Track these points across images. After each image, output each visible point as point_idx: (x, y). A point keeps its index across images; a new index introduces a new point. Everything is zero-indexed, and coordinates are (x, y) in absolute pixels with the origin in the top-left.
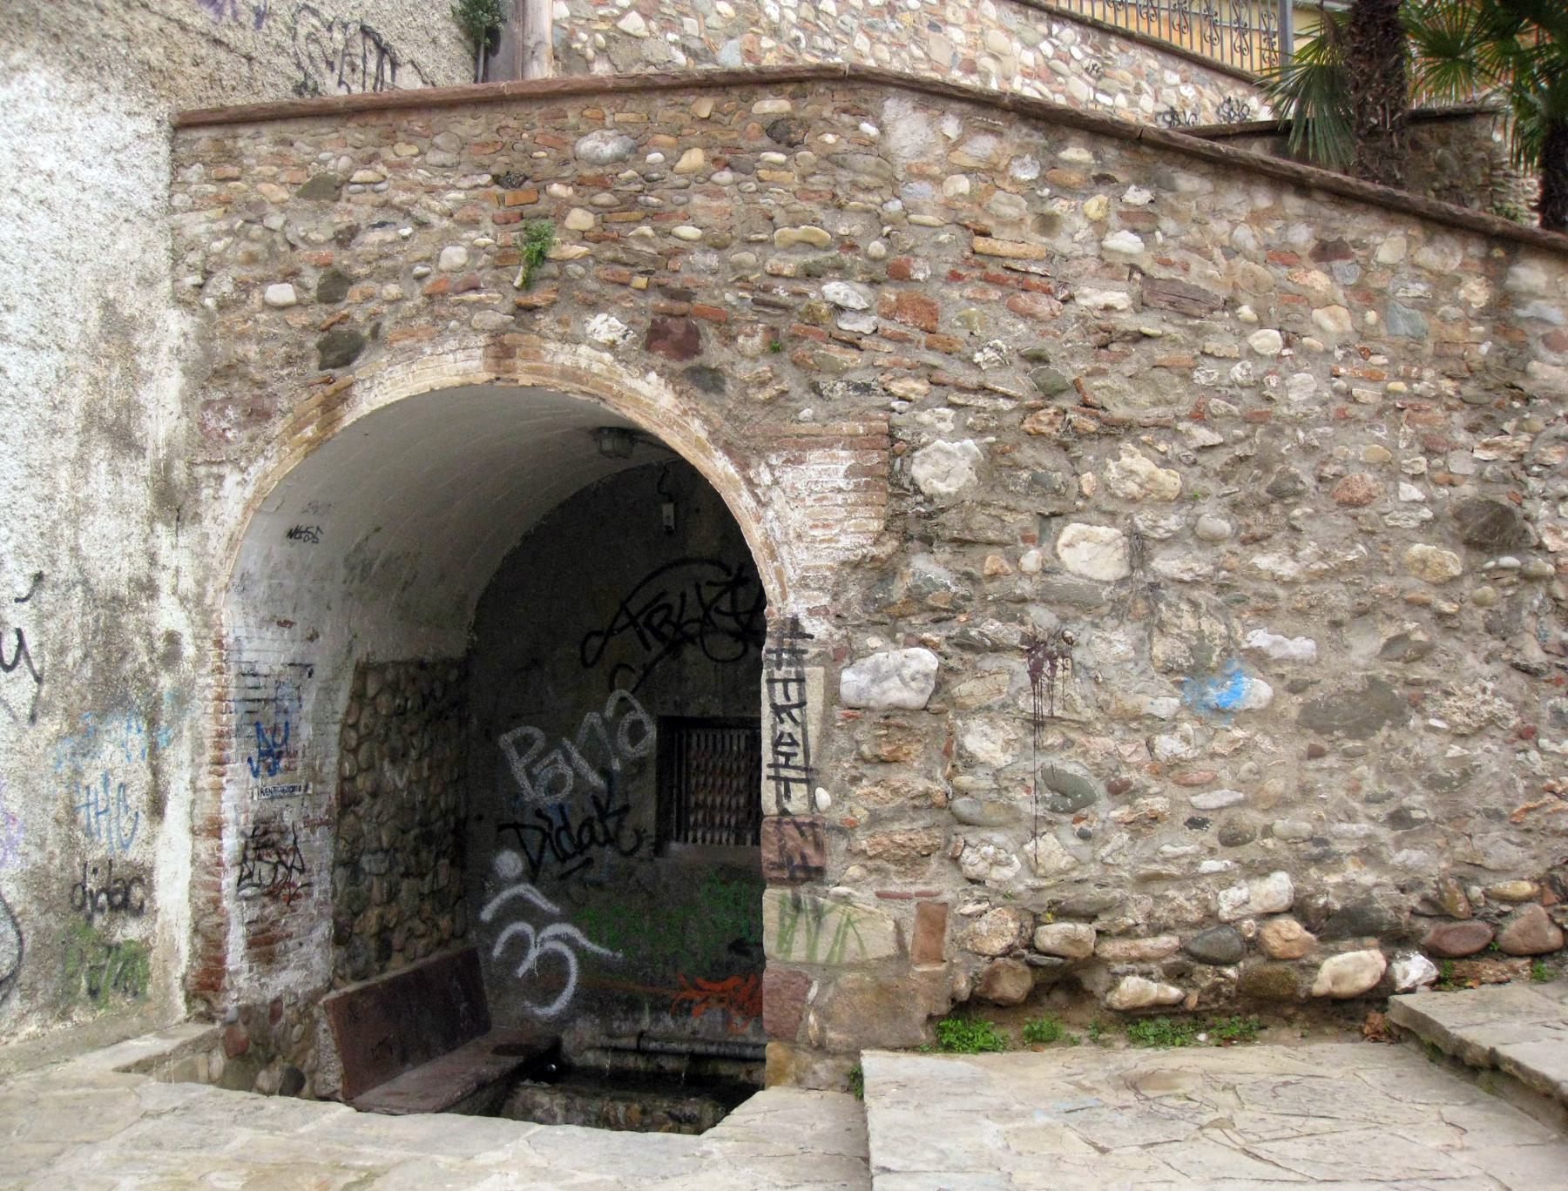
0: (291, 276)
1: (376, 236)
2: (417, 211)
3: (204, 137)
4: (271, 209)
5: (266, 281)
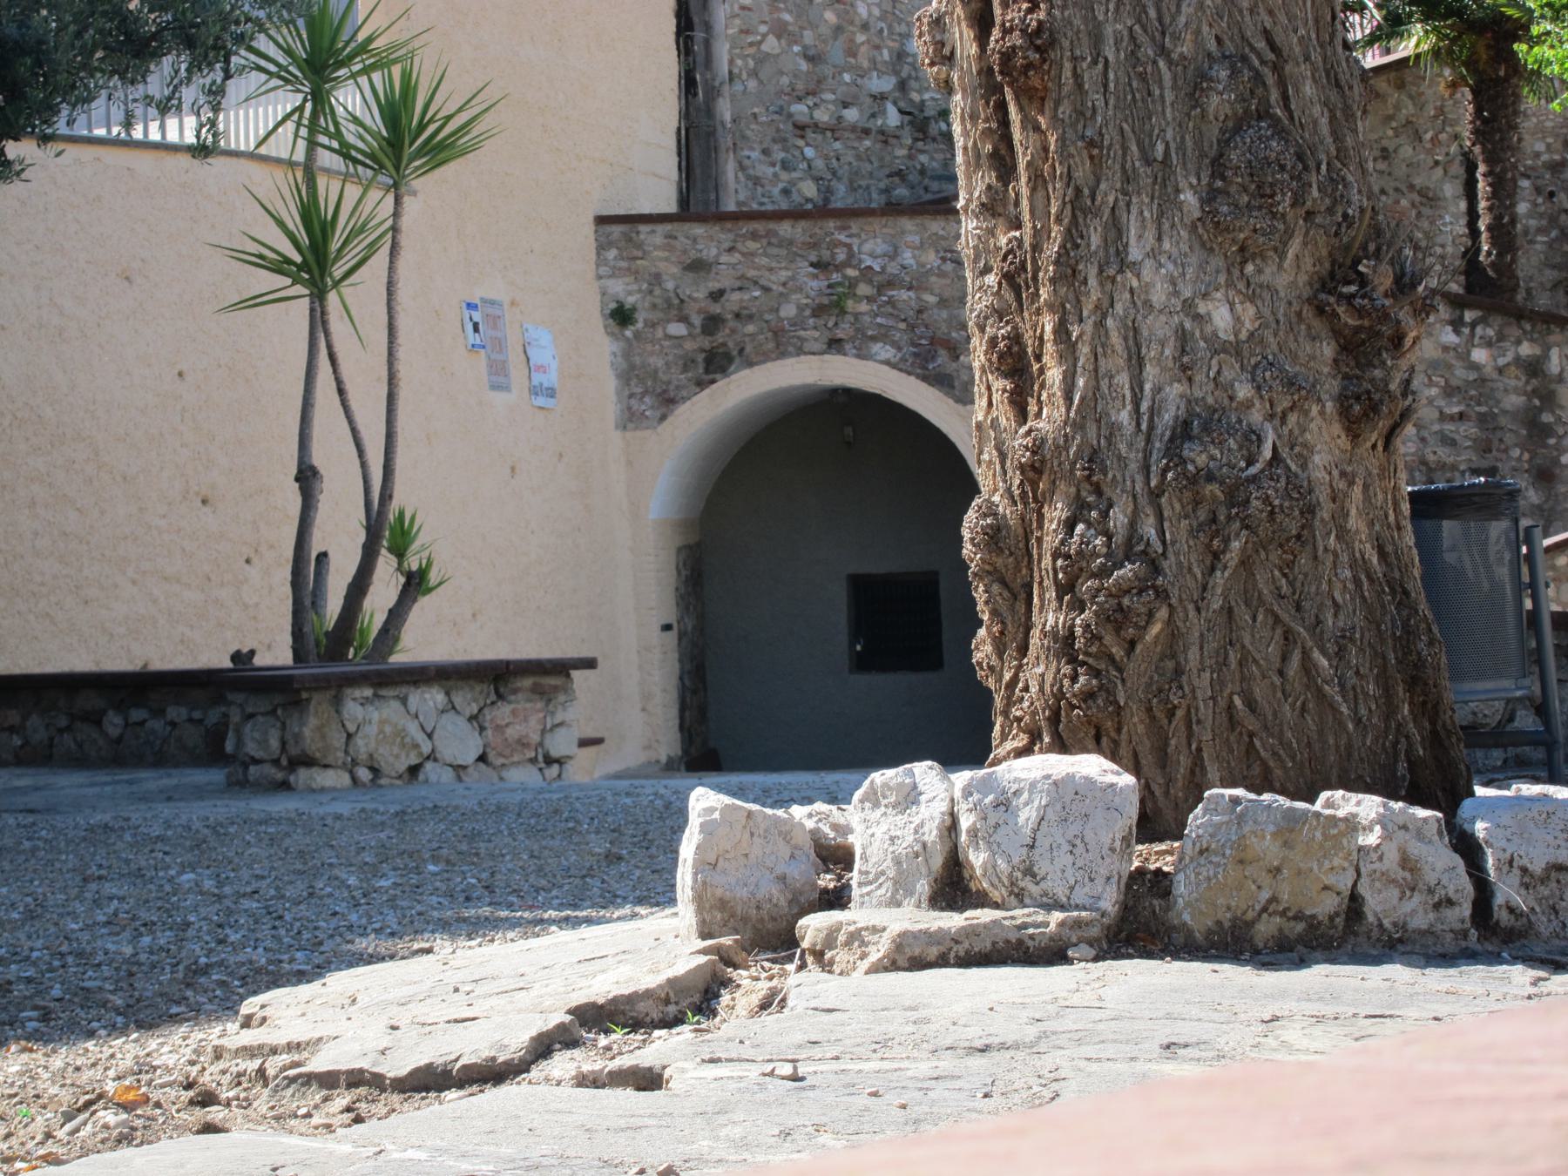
0: (684, 319)
1: (736, 296)
2: (763, 282)
3: (616, 230)
4: (665, 277)
5: (669, 321)
